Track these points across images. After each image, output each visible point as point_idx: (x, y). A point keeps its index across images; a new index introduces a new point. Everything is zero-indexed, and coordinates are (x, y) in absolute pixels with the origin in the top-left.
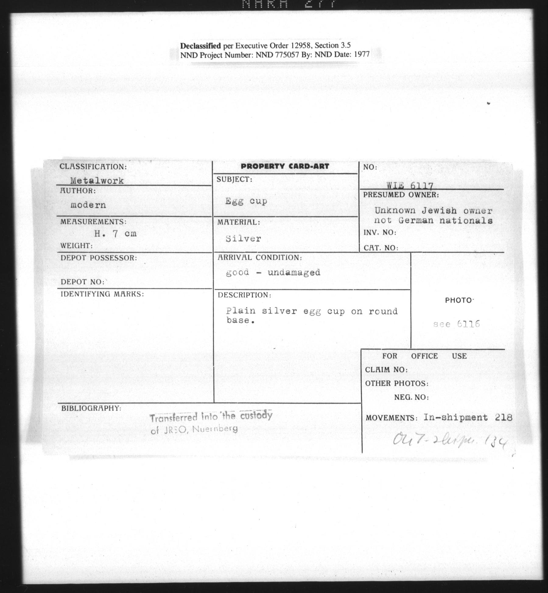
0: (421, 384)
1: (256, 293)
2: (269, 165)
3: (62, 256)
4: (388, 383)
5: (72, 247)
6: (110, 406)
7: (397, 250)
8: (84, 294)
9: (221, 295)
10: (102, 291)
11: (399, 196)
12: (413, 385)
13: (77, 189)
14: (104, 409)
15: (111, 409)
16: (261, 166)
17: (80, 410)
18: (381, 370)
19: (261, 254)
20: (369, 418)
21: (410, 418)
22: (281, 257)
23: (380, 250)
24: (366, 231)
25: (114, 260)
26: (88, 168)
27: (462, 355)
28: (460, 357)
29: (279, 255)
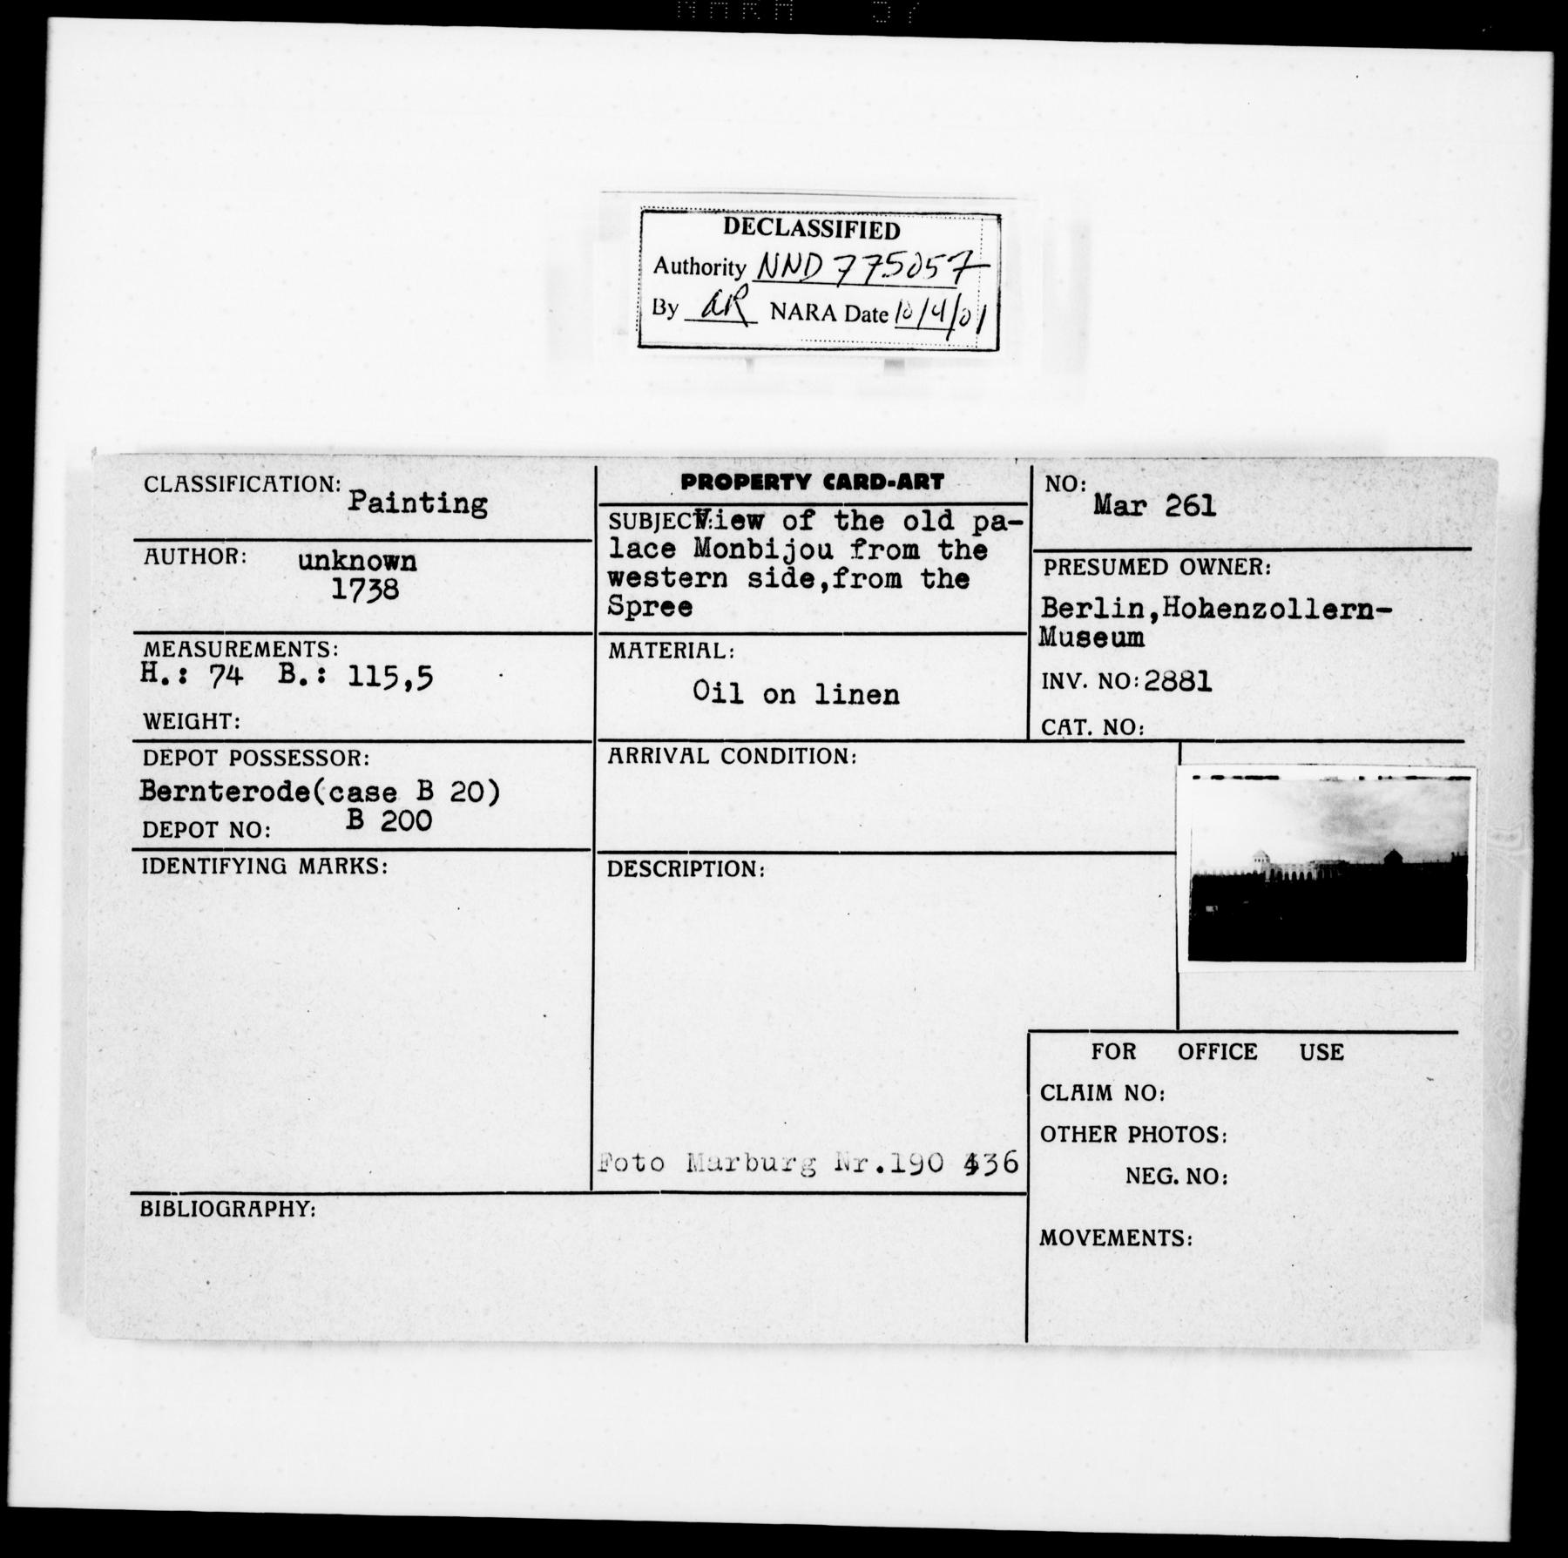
0: (1207, 1136)
1: (720, 863)
2: (763, 479)
3: (146, 752)
4: (1111, 1132)
5: (177, 725)
6: (282, 1203)
7: (1141, 733)
8: (209, 866)
10: (262, 855)
11: (1152, 571)
12: (1181, 1140)
13: (194, 550)
14: (263, 1211)
15: (287, 1212)
16: (741, 480)
17: (194, 1215)
18: (1086, 1096)
19: (737, 746)
20: (1048, 1238)
21: (1170, 1238)
22: (796, 755)
23: (1090, 733)
24: (1049, 677)
26: (225, 487)
27: (1329, 1050)
28: (1323, 1056)
29: (791, 750)
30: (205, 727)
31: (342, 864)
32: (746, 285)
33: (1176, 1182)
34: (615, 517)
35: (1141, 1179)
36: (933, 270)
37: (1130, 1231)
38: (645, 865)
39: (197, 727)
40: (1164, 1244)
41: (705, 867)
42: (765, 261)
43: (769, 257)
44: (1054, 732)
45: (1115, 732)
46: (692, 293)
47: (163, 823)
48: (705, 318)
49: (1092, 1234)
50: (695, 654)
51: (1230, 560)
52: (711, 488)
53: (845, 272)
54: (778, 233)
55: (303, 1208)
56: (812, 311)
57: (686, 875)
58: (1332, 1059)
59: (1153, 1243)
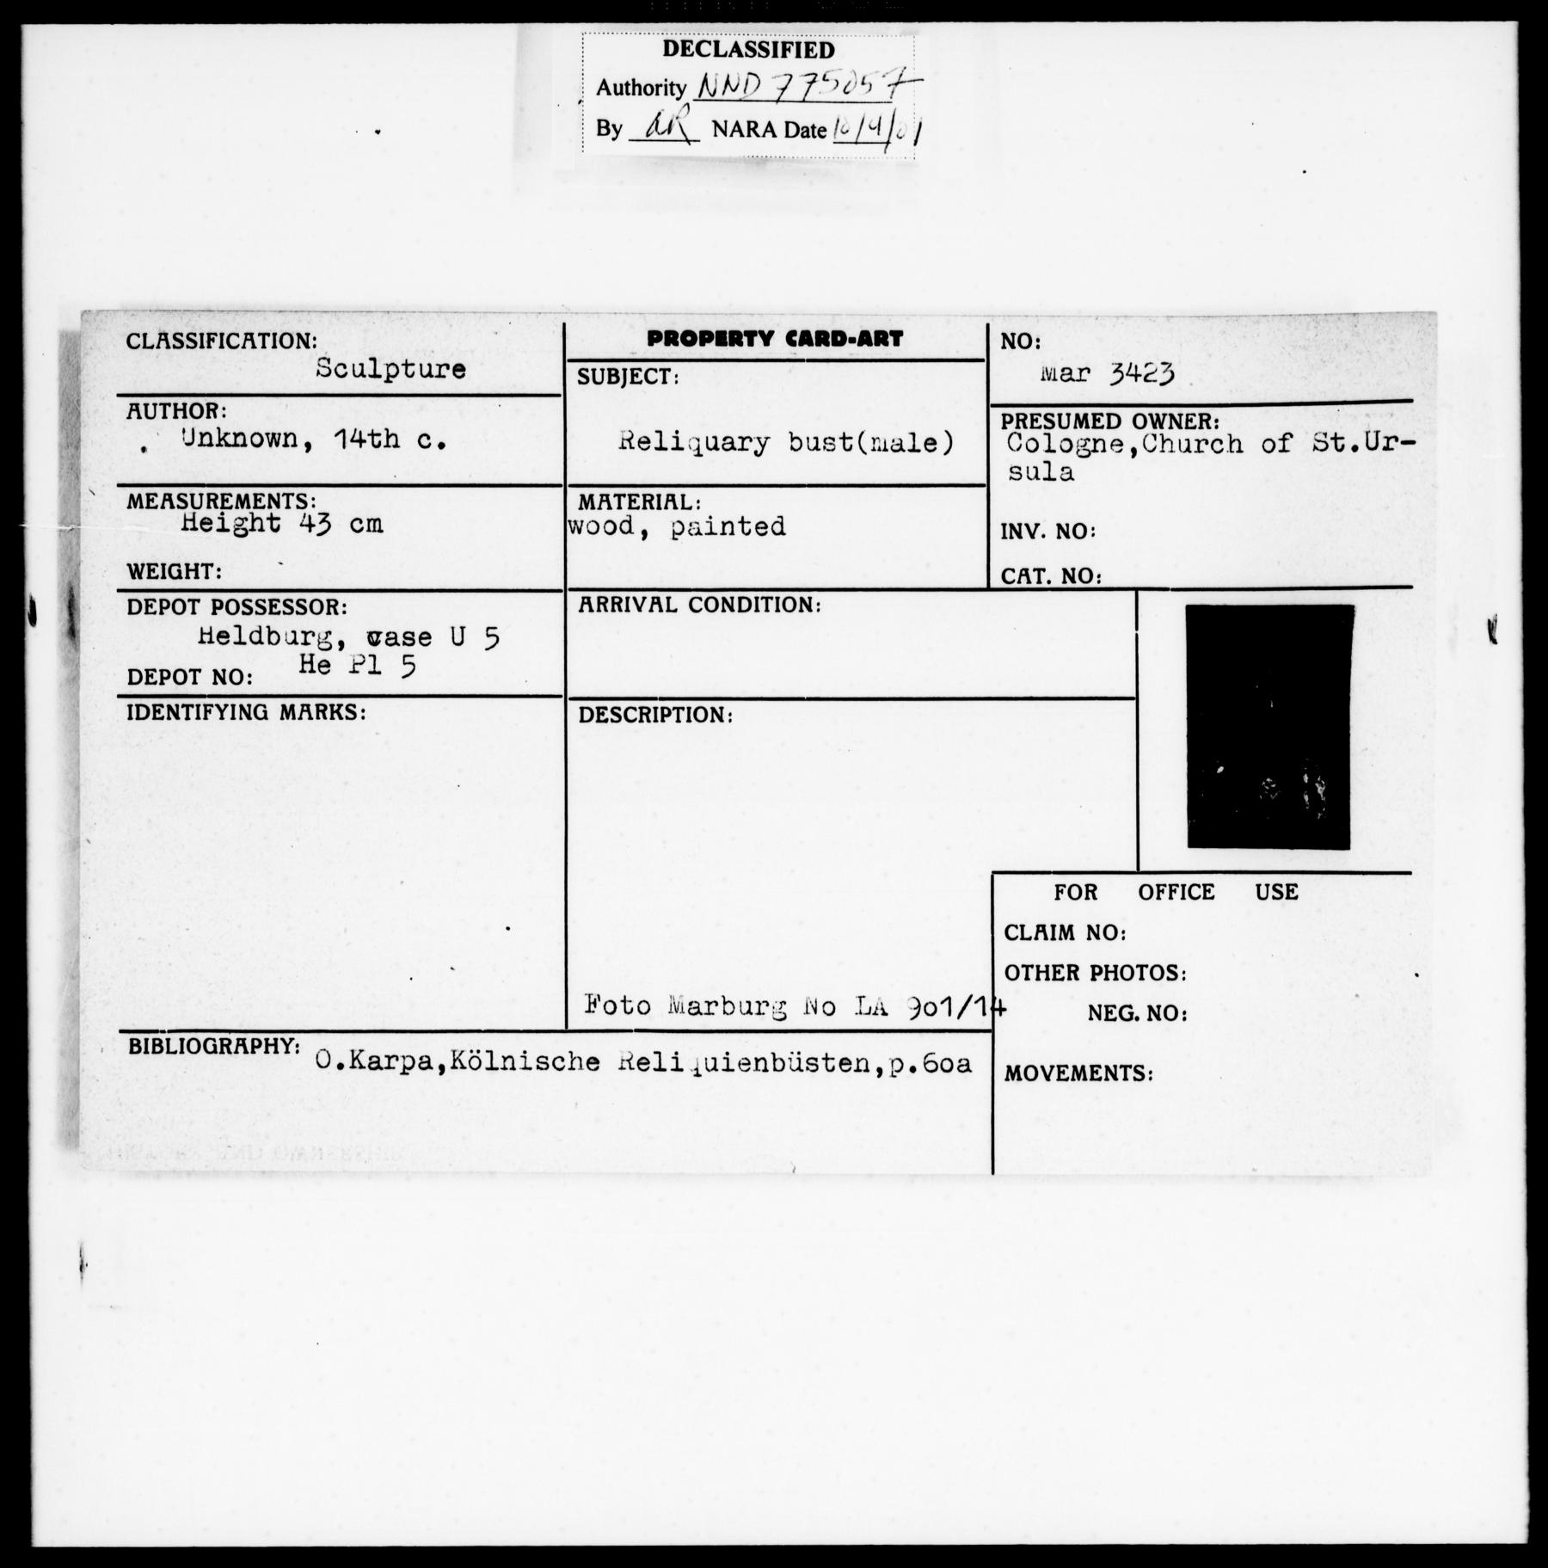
0: (1167, 974)
1: (689, 709)
2: (728, 335)
3: (130, 601)
4: (1073, 971)
5: (161, 575)
6: (267, 1040)
7: (1099, 582)
8: (193, 712)
9: (587, 715)
10: (245, 702)
11: (1106, 426)
12: (1142, 978)
13: (176, 405)
14: (249, 1048)
15: (271, 1049)
16: (706, 337)
17: (182, 1052)
18: (1049, 935)
19: (704, 595)
20: (1013, 1073)
21: (1131, 1073)
22: (762, 604)
24: (1008, 528)
25: (282, 613)
26: (205, 344)
27: (1284, 890)
28: (1278, 895)
29: (757, 598)
30: (188, 577)
31: (321, 710)
32: (688, 104)
33: (1137, 1019)
34: (583, 372)
35: (1103, 1016)
36: (867, 87)
37: (1092, 1067)
38: (616, 711)
39: (180, 577)
40: (1126, 1079)
41: (674, 713)
42: (705, 81)
43: (708, 77)
44: (1014, 581)
45: (1073, 581)
46: (634, 113)
47: (147, 671)
48: (650, 138)
49: (1055, 1069)
50: (663, 505)
51: (1180, 415)
52: (676, 344)
53: (784, 89)
54: (717, 54)
55: (287, 1046)
56: (752, 128)
57: (656, 721)
58: (1287, 898)
59: (1115, 1078)
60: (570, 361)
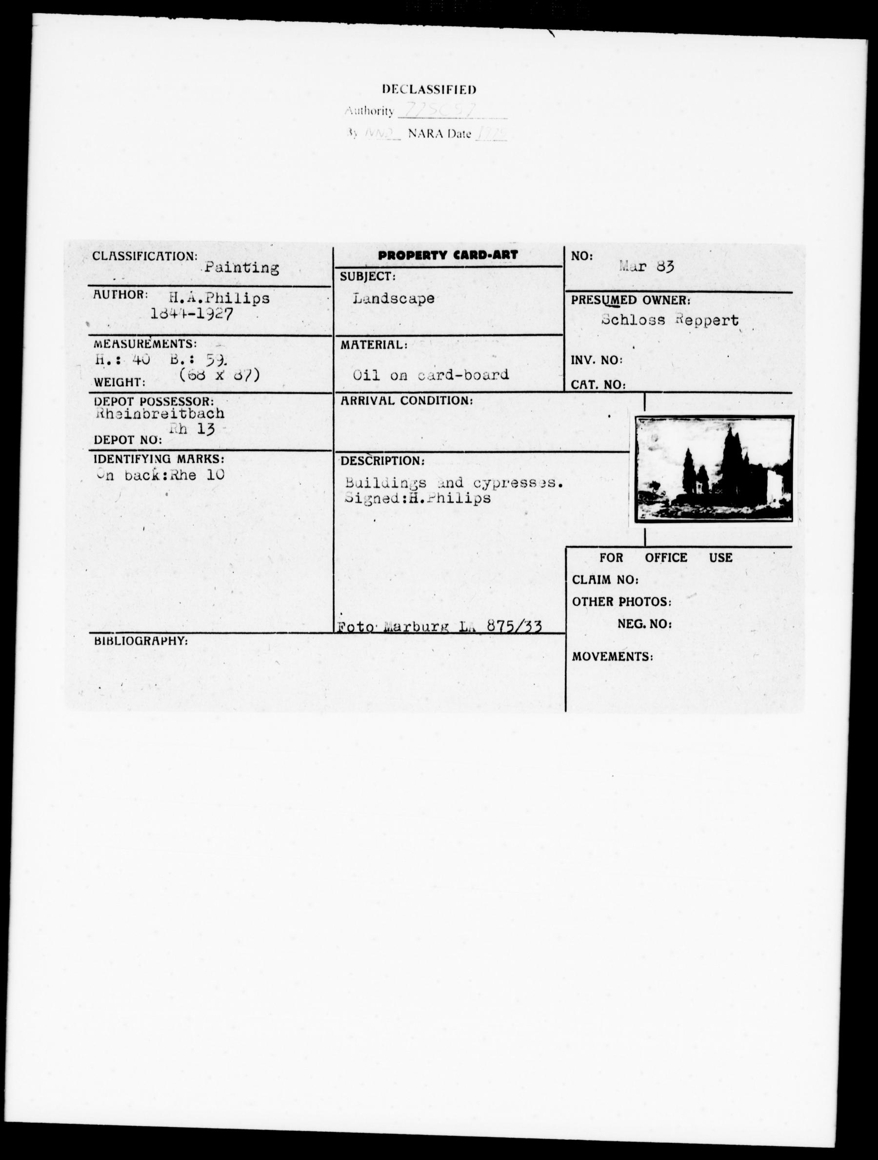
0: (661, 602)
2: (422, 254)
4: (610, 601)
5: (112, 384)
6: (170, 638)
8: (130, 459)
9: (345, 461)
10: (158, 453)
12: (647, 605)
15: (172, 642)
16: (410, 254)
18: (597, 581)
20: (577, 656)
24: (575, 358)
27: (725, 557)
29: (438, 397)
40: (638, 660)
41: (393, 460)
45: (610, 387)
52: (394, 258)
57: (383, 464)
59: (632, 659)
60: (337, 268)
